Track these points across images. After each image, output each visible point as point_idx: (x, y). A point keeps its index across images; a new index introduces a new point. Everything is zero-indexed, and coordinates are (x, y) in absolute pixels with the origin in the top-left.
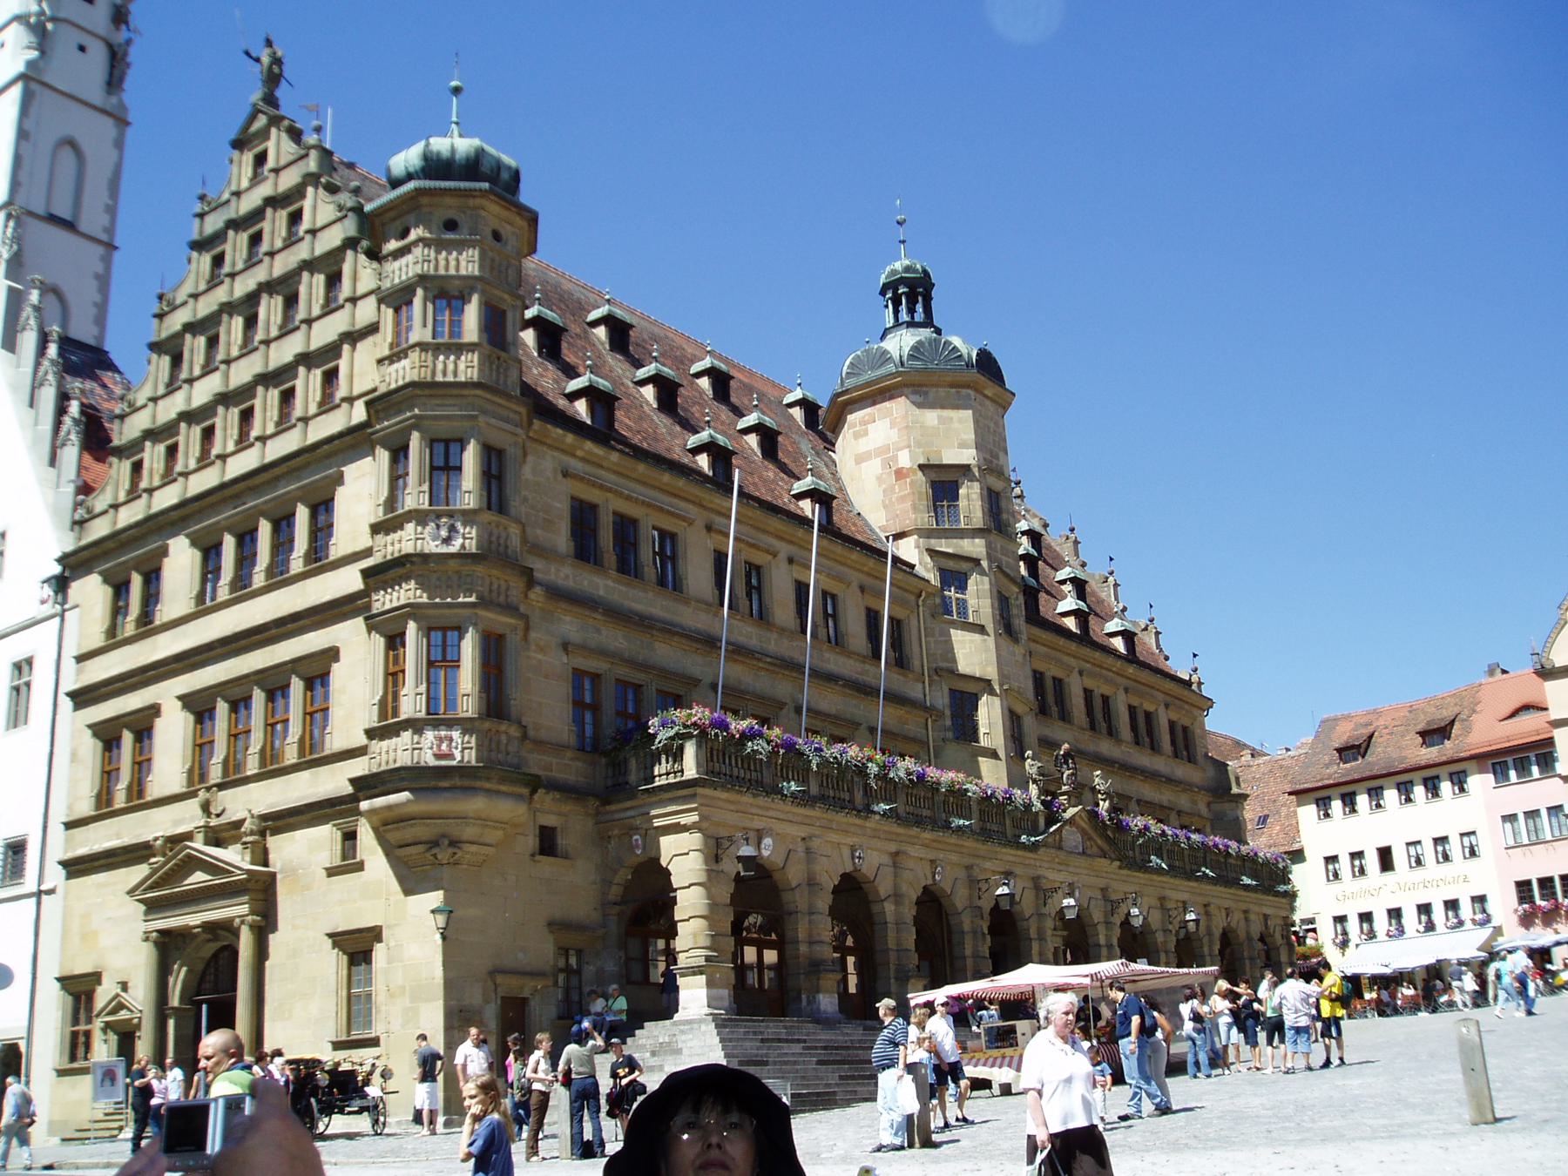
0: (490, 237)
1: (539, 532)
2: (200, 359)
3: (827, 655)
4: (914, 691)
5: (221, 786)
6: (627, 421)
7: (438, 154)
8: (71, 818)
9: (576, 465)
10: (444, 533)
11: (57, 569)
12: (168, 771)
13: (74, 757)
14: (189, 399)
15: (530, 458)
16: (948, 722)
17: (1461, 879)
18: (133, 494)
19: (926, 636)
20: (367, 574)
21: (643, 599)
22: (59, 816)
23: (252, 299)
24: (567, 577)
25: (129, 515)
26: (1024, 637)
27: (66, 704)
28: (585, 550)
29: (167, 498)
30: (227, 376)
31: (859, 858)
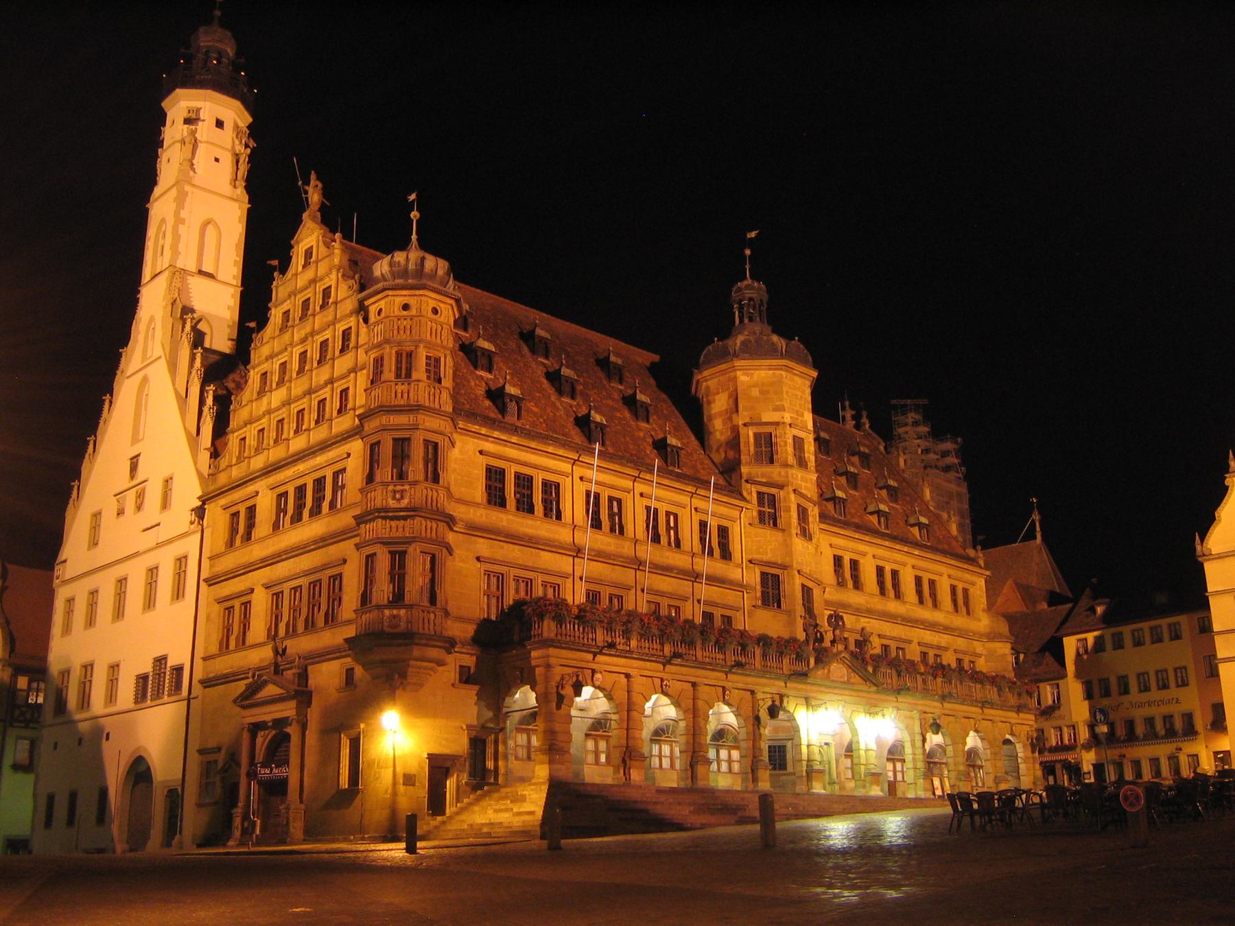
0: (430, 312)
1: (463, 489)
2: (276, 378)
3: (667, 554)
4: (735, 574)
5: (283, 639)
6: (535, 409)
7: (399, 262)
8: (207, 655)
9: (489, 446)
10: (398, 496)
11: (201, 503)
12: (258, 628)
13: (208, 618)
14: (269, 403)
15: (458, 444)
16: (759, 594)
17: (1174, 701)
18: (240, 459)
19: (745, 537)
20: (355, 517)
21: (535, 526)
22: (199, 653)
23: (303, 341)
24: (481, 515)
25: (236, 473)
26: (817, 535)
27: (203, 585)
28: (496, 497)
29: (258, 462)
30: (289, 389)
31: (666, 685)
